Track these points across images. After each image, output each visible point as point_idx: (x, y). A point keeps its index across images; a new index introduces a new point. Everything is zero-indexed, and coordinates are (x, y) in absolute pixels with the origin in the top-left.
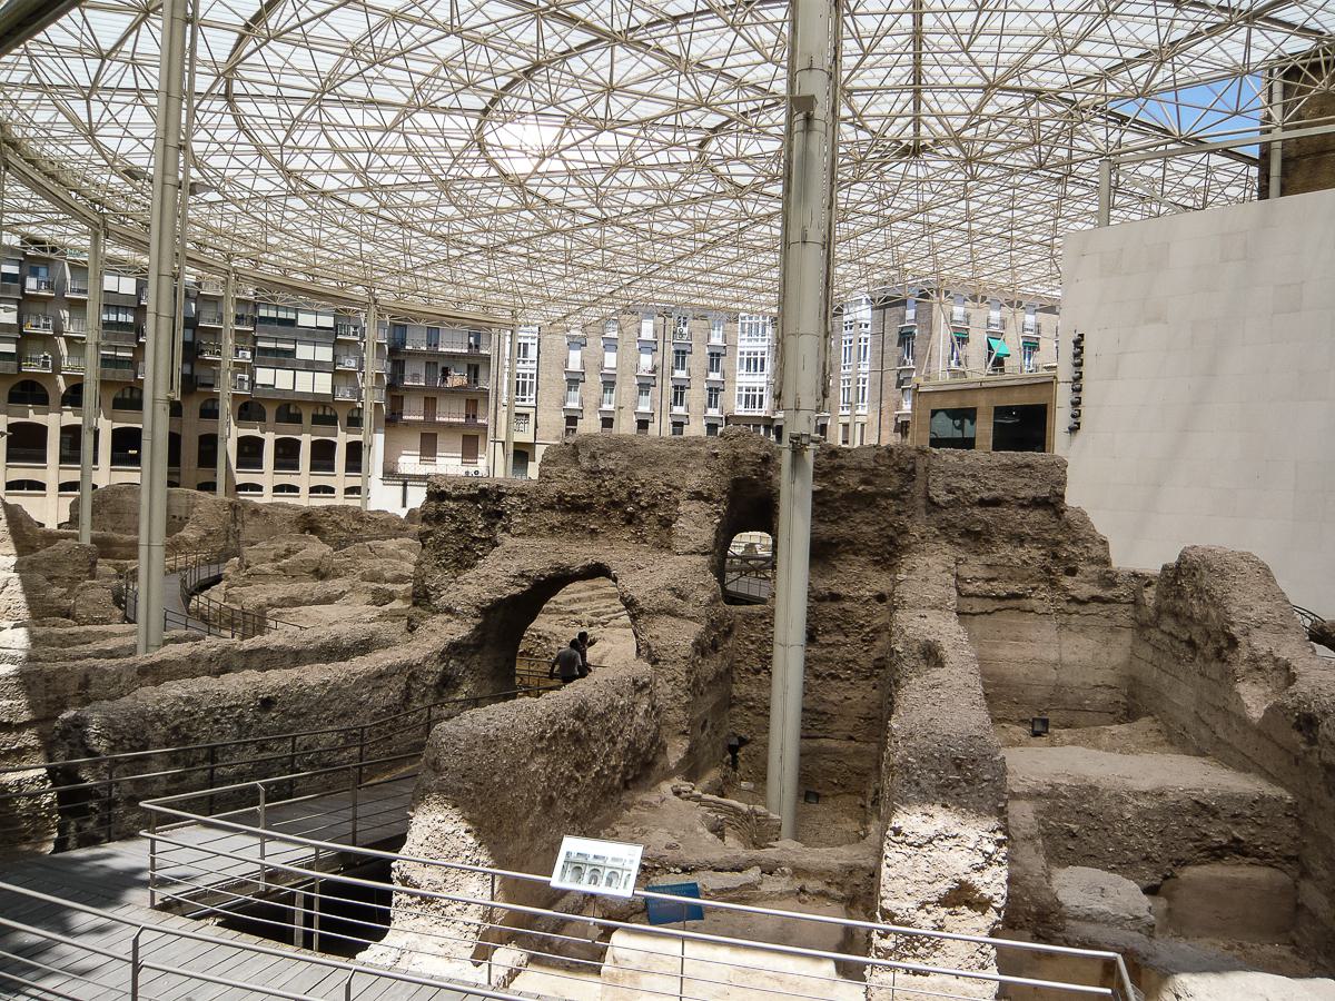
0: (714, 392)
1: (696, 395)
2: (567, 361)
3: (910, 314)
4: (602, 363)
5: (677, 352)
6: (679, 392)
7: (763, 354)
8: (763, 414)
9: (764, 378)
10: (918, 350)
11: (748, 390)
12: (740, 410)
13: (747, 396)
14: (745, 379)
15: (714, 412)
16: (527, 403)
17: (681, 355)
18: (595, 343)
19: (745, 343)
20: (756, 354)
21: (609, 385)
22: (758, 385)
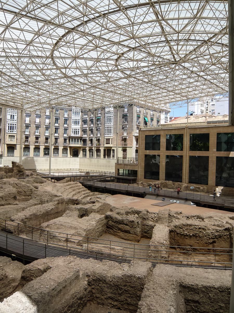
0: (66, 130)
1: (61, 131)
2: (25, 120)
3: (126, 110)
4: (35, 121)
5: (56, 119)
6: (57, 129)
7: (79, 120)
8: (79, 136)
9: (80, 126)
10: (129, 119)
11: (75, 129)
12: (73, 135)
13: (75, 131)
14: (74, 126)
15: (65, 135)
16: (14, 132)
17: (57, 120)
18: (34, 116)
19: (74, 117)
20: (77, 120)
21: (38, 127)
22: (78, 128)
